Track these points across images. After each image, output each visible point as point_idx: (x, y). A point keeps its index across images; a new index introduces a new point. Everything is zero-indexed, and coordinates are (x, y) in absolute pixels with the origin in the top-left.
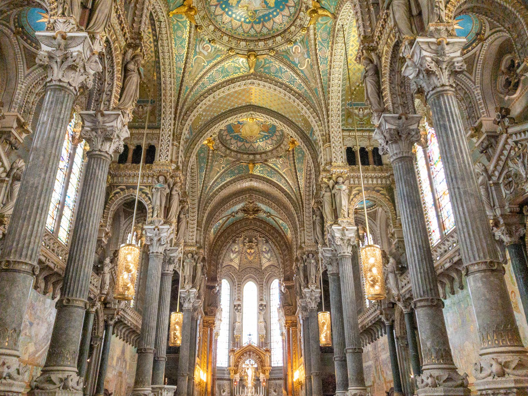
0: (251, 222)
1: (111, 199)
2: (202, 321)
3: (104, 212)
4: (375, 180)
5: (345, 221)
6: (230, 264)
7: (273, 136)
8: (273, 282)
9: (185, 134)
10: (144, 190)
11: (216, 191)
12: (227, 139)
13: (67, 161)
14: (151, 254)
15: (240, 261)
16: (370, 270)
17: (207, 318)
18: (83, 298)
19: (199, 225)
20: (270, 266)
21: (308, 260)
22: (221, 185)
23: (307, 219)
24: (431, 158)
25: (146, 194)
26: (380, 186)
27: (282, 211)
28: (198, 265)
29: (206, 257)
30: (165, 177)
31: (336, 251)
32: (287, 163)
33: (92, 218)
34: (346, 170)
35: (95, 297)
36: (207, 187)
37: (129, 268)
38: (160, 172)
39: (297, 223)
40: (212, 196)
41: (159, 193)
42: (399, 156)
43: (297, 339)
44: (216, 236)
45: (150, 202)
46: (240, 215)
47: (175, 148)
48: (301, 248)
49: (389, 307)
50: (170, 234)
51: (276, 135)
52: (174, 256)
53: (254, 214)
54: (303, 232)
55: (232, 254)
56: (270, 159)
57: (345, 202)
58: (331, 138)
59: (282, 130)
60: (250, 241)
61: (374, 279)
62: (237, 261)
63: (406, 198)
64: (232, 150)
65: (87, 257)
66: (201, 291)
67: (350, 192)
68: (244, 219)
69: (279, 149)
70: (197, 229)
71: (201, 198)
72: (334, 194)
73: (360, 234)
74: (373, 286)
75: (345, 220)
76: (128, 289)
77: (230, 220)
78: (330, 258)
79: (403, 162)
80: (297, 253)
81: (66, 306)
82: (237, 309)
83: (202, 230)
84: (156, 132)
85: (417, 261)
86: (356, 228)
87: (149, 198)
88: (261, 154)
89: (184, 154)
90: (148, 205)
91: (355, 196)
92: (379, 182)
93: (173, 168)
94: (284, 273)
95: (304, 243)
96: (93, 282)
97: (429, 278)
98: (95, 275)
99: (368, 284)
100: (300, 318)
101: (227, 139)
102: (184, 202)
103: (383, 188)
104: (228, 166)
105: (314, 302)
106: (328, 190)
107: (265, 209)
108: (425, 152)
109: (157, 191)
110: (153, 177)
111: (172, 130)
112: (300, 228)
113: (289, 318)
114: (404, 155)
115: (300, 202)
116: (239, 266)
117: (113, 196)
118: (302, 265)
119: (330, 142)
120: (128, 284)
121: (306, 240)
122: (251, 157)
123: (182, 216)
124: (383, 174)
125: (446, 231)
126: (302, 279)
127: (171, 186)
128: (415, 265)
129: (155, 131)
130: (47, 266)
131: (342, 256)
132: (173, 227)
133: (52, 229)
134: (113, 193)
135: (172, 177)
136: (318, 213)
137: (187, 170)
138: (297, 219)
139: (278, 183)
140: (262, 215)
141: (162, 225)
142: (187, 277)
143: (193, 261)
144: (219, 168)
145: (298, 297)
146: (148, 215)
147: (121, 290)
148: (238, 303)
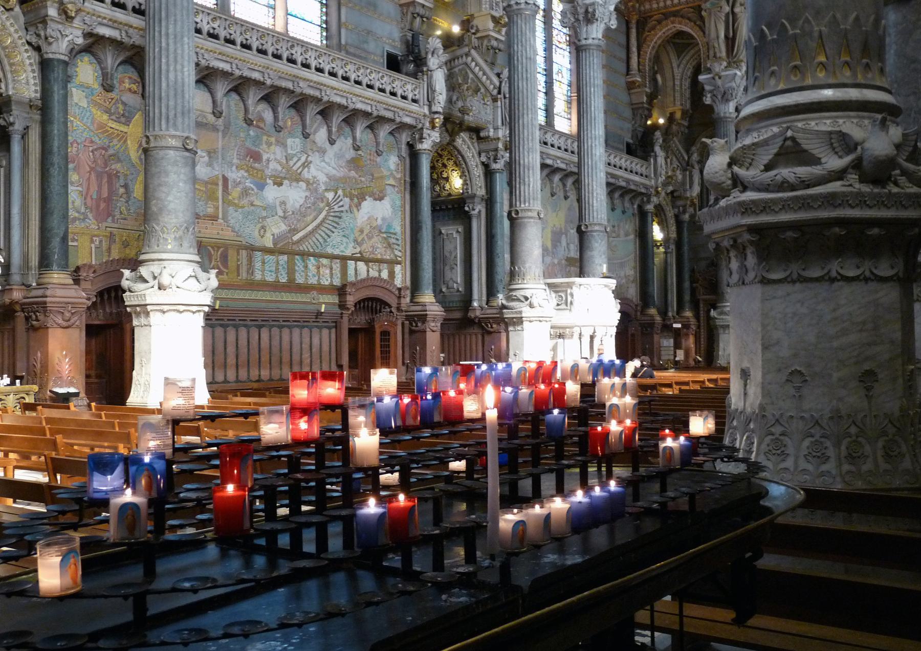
65: (167, 50)
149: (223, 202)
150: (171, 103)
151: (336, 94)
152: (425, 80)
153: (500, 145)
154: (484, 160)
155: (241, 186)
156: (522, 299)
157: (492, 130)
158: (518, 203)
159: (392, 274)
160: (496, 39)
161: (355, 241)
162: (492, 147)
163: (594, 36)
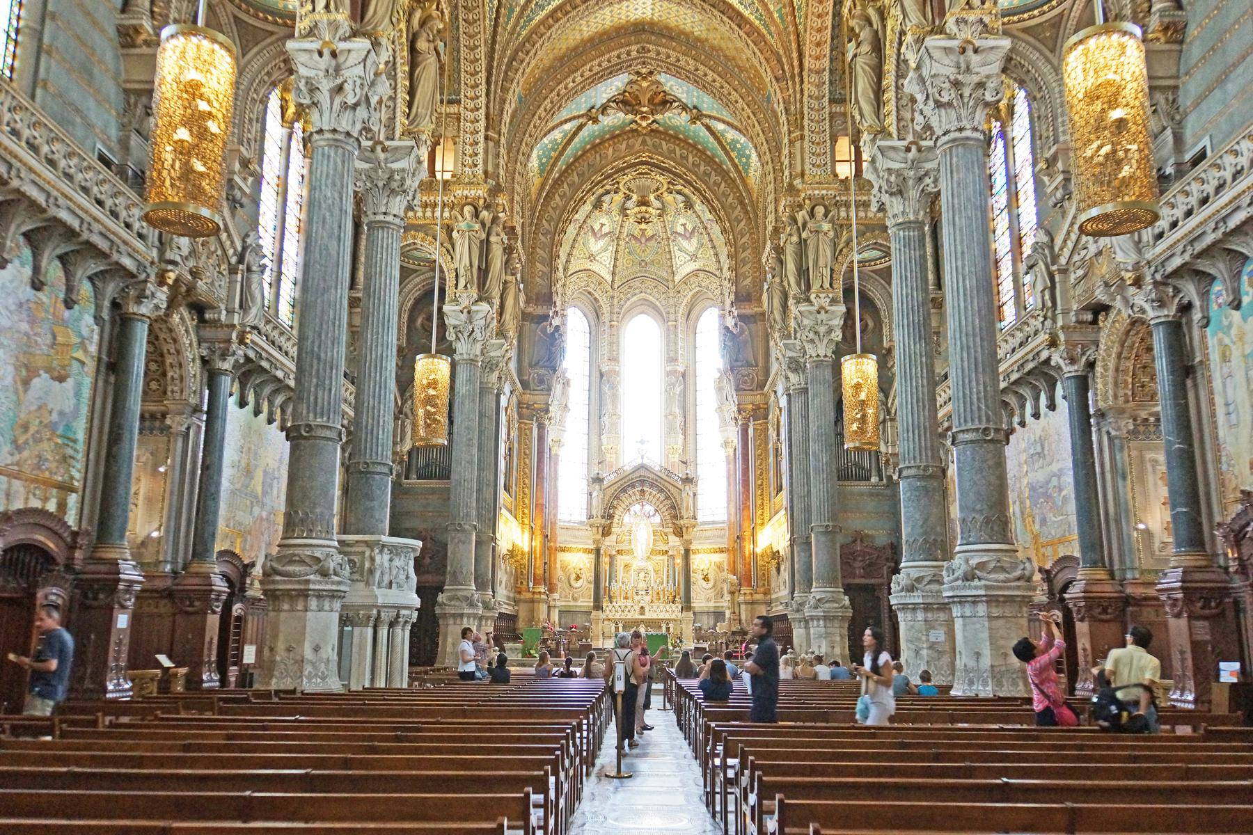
0: (644, 143)
2: (514, 400)
6: (588, 265)
11: (538, 26)
14: (316, 137)
15: (616, 259)
20: (695, 273)
21: (810, 225)
23: (814, 103)
27: (735, 96)
28: (493, 239)
40: (528, 39)
46: (615, 118)
52: (403, 170)
54: (798, 144)
55: (592, 240)
60: (643, 203)
62: (606, 258)
66: (508, 316)
70: (486, 138)
71: (494, 42)
75: (972, 17)
77: (584, 133)
78: (899, 173)
95: (803, 175)
96: (123, 214)
100: (780, 389)
105: (825, 341)
112: (790, 132)
113: (748, 398)
115: (795, 55)
116: (613, 273)
118: (795, 239)
121: (807, 167)
123: (422, 45)
126: (792, 280)
131: (954, 140)
136: (865, 34)
138: (780, 108)
140: (675, 119)
141: (345, 39)
142: (462, 272)
143: (477, 227)
151: (33, 182)
153: (234, 336)
154: (205, 353)
156: (308, 560)
157: (224, 312)
159: (62, 506)
160: (240, 189)
161: (14, 442)
162: (221, 334)
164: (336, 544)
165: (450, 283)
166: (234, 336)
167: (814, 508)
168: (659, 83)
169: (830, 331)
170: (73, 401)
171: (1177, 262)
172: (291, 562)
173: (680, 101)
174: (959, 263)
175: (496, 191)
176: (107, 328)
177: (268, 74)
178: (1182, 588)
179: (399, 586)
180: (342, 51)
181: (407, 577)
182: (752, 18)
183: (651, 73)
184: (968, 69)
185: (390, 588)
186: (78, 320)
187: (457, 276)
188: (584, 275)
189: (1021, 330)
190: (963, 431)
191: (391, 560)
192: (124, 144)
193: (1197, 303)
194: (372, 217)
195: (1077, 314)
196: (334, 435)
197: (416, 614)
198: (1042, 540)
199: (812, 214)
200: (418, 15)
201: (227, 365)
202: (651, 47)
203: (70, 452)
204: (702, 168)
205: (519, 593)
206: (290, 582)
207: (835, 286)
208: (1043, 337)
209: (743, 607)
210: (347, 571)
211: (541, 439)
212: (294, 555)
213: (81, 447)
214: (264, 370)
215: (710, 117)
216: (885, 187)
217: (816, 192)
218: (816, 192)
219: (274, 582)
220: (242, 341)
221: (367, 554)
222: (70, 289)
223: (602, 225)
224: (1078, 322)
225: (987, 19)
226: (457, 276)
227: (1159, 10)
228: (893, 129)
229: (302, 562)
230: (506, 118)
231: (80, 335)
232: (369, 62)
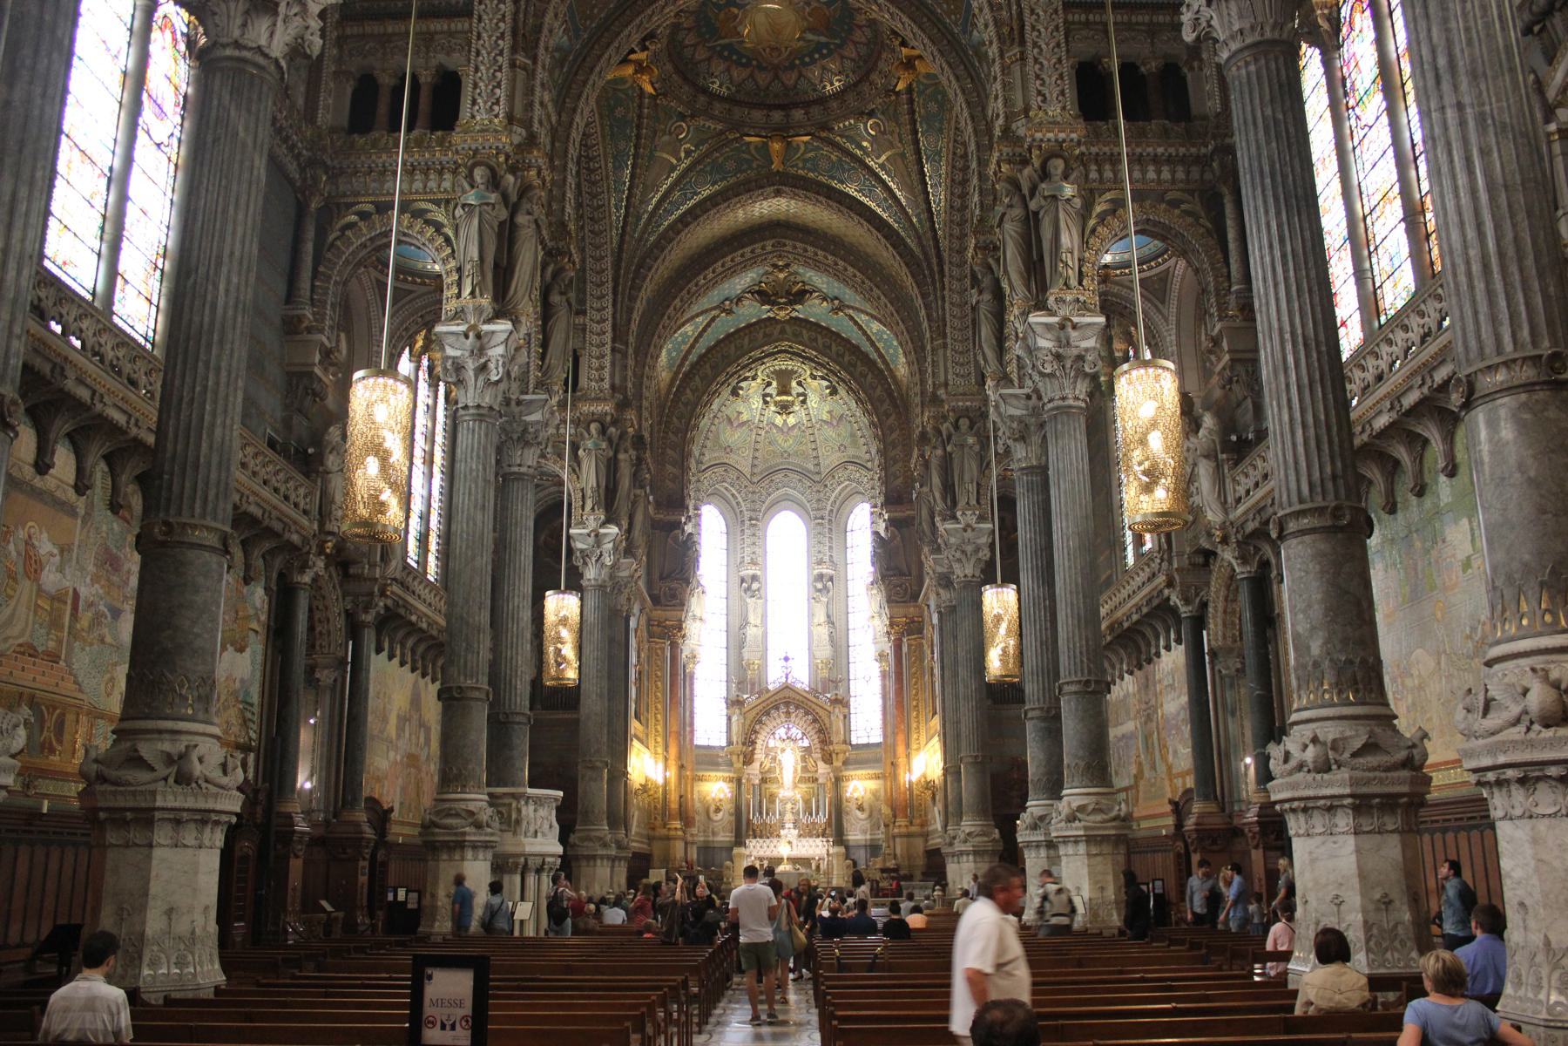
0: (783, 331)
1: (332, 245)
2: (643, 621)
3: (313, 287)
4: (1165, 169)
5: (1069, 298)
7: (840, 46)
8: (856, 511)
9: (551, 31)
10: (429, 216)
11: (666, 230)
12: (697, 57)
13: (179, 120)
14: (461, 412)
16: (1143, 442)
17: (658, 613)
18: (215, 519)
19: (619, 335)
20: (844, 465)
22: (683, 208)
23: (956, 311)
24: (1348, 85)
25: (438, 227)
26: (1181, 185)
27: (876, 291)
28: (622, 456)
29: (646, 435)
30: (492, 169)
31: (1040, 398)
32: (892, 133)
33: (225, 269)
34: (1074, 136)
35: (305, 540)
36: (639, 218)
37: (380, 445)
38: (476, 151)
39: (925, 324)
40: (657, 242)
41: (476, 222)
42: (1249, 41)
43: (922, 668)
44: (676, 373)
45: (449, 250)
46: (752, 311)
47: (521, 74)
48: (935, 400)
49: (1193, 565)
50: (516, 350)
51: (855, 43)
52: (538, 422)
53: (790, 303)
54: (941, 352)
56: (838, 119)
57: (1069, 239)
58: (1028, 28)
59: (873, 23)
60: (784, 390)
61: (1154, 466)
63: (1268, 181)
64: (714, 97)
65: (216, 393)
66: (637, 532)
67: (1088, 206)
68: (760, 321)
69: (865, 87)
70: (613, 350)
72: (1036, 214)
73: (1117, 354)
74: (1148, 489)
76: (381, 507)
78: (1020, 420)
79: (1263, 62)
80: (923, 419)
81: (163, 544)
82: (749, 588)
83: (630, 351)
84: (460, 26)
85: (1294, 389)
86: (1102, 320)
87: (448, 240)
88: (807, 105)
89: (555, 102)
90: (444, 261)
91: (1102, 218)
92: (1180, 175)
93: (517, 140)
94: (886, 481)
95: (946, 385)
96: (293, 497)
97: (1330, 442)
98: (300, 478)
99: (1135, 484)
100: (933, 607)
101: (697, 57)
102: (561, 253)
103: (1191, 192)
104: (703, 148)
106: (1016, 199)
107: (824, 287)
108: (1328, 64)
109: (470, 214)
110: (455, 172)
111: (508, 18)
113: (900, 611)
114: (1268, 35)
115: (934, 261)
116: (754, 466)
117: (335, 239)
118: (939, 452)
119: (1022, 42)
120: (381, 492)
122: (777, 116)
123: (555, 298)
124: (1193, 150)
125: (1383, 319)
126: (937, 495)
127: (514, 198)
128: (1289, 401)
129: (460, 25)
130: (135, 439)
131: (1057, 408)
132: (523, 330)
133: (151, 334)
134: (338, 226)
135: (513, 170)
136: (986, 282)
137: (566, 151)
138: (923, 313)
139: (863, 199)
141: (489, 321)
143: (604, 445)
144: (676, 155)
145: (926, 549)
146: (447, 294)
147: (363, 512)
148: (751, 572)
149: (69, 633)
150: (213, 476)
152: (319, 483)
153: (376, 589)
155: (93, 609)
156: (463, 814)
158: (462, 678)
163: (530, 463)
164: (486, 797)
165: (576, 504)
166: (376, 589)
167: (963, 736)
168: (796, 273)
169: (977, 549)
170: (250, 668)
171: (1251, 526)
172: (449, 815)
173: (820, 291)
174: (1064, 524)
175: (622, 406)
176: (274, 596)
177: (406, 329)
178: (1257, 822)
179: (544, 835)
180: (487, 333)
181: (551, 827)
182: (891, 221)
183: (787, 266)
184: (1068, 343)
185: (536, 837)
186: (253, 594)
187: (583, 496)
188: (720, 470)
189: (1149, 566)
190: (1068, 683)
191: (535, 811)
192: (287, 424)
193: (1273, 561)
194: (507, 470)
195: (1189, 558)
196: (483, 696)
197: (559, 861)
198: (1174, 771)
199: (956, 427)
200: (550, 269)
201: (369, 617)
202: (787, 242)
203: (248, 715)
204: (847, 358)
205: (653, 829)
206: (449, 834)
207: (982, 502)
208: (1161, 579)
209: (898, 840)
210: (496, 824)
211: (674, 658)
212: (450, 809)
213: (256, 709)
214: (401, 617)
215: (852, 308)
216: (1008, 434)
217: (960, 404)
218: (960, 404)
219: (433, 834)
220: (383, 594)
221: (514, 805)
222: (248, 567)
223: (740, 413)
224: (1190, 564)
225: (1082, 298)
226: (583, 496)
227: (1236, 291)
228: (1014, 377)
229: (457, 815)
230: (634, 327)
231: (256, 609)
232: (510, 343)
